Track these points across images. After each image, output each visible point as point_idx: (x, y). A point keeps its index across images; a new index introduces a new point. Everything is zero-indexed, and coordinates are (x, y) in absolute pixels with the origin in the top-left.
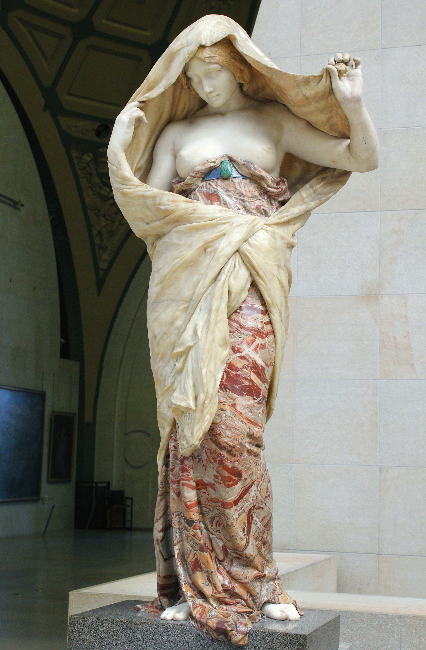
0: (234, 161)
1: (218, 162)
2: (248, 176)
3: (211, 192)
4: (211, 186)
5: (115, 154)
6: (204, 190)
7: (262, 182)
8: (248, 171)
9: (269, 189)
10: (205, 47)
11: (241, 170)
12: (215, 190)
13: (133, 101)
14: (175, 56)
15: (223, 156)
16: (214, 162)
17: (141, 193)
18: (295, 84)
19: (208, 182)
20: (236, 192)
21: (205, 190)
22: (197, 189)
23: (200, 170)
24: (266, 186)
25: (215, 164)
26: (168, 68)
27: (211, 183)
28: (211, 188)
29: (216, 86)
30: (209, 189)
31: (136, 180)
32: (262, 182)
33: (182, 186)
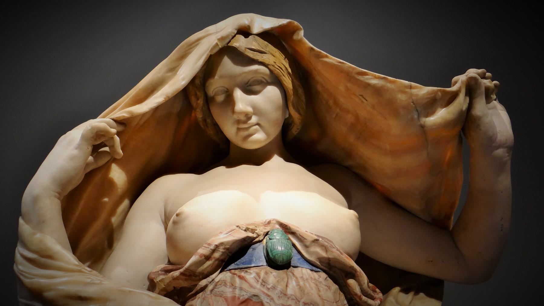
0: (293, 233)
1: (261, 230)
2: (322, 267)
3: (246, 297)
4: (246, 281)
5: (35, 200)
6: (228, 292)
7: (351, 282)
8: (324, 254)
9: (364, 298)
10: (251, 34)
11: (308, 252)
12: (255, 292)
13: (104, 117)
14: (191, 48)
15: (269, 223)
16: (253, 231)
17: (73, 289)
18: (411, 100)
19: (237, 272)
20: (303, 300)
21: (231, 290)
22: (210, 287)
23: (222, 244)
24: (357, 290)
25: (255, 235)
26: (178, 66)
27: (243, 274)
28: (245, 286)
29: (257, 110)
30: (241, 289)
31: (68, 257)
32: (351, 282)
33: (175, 279)
